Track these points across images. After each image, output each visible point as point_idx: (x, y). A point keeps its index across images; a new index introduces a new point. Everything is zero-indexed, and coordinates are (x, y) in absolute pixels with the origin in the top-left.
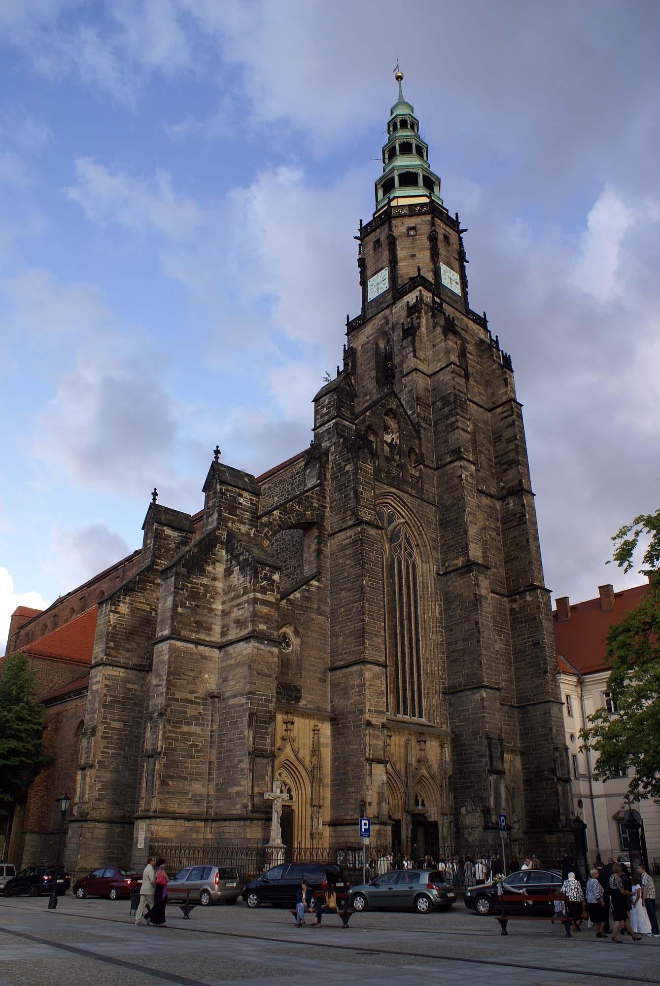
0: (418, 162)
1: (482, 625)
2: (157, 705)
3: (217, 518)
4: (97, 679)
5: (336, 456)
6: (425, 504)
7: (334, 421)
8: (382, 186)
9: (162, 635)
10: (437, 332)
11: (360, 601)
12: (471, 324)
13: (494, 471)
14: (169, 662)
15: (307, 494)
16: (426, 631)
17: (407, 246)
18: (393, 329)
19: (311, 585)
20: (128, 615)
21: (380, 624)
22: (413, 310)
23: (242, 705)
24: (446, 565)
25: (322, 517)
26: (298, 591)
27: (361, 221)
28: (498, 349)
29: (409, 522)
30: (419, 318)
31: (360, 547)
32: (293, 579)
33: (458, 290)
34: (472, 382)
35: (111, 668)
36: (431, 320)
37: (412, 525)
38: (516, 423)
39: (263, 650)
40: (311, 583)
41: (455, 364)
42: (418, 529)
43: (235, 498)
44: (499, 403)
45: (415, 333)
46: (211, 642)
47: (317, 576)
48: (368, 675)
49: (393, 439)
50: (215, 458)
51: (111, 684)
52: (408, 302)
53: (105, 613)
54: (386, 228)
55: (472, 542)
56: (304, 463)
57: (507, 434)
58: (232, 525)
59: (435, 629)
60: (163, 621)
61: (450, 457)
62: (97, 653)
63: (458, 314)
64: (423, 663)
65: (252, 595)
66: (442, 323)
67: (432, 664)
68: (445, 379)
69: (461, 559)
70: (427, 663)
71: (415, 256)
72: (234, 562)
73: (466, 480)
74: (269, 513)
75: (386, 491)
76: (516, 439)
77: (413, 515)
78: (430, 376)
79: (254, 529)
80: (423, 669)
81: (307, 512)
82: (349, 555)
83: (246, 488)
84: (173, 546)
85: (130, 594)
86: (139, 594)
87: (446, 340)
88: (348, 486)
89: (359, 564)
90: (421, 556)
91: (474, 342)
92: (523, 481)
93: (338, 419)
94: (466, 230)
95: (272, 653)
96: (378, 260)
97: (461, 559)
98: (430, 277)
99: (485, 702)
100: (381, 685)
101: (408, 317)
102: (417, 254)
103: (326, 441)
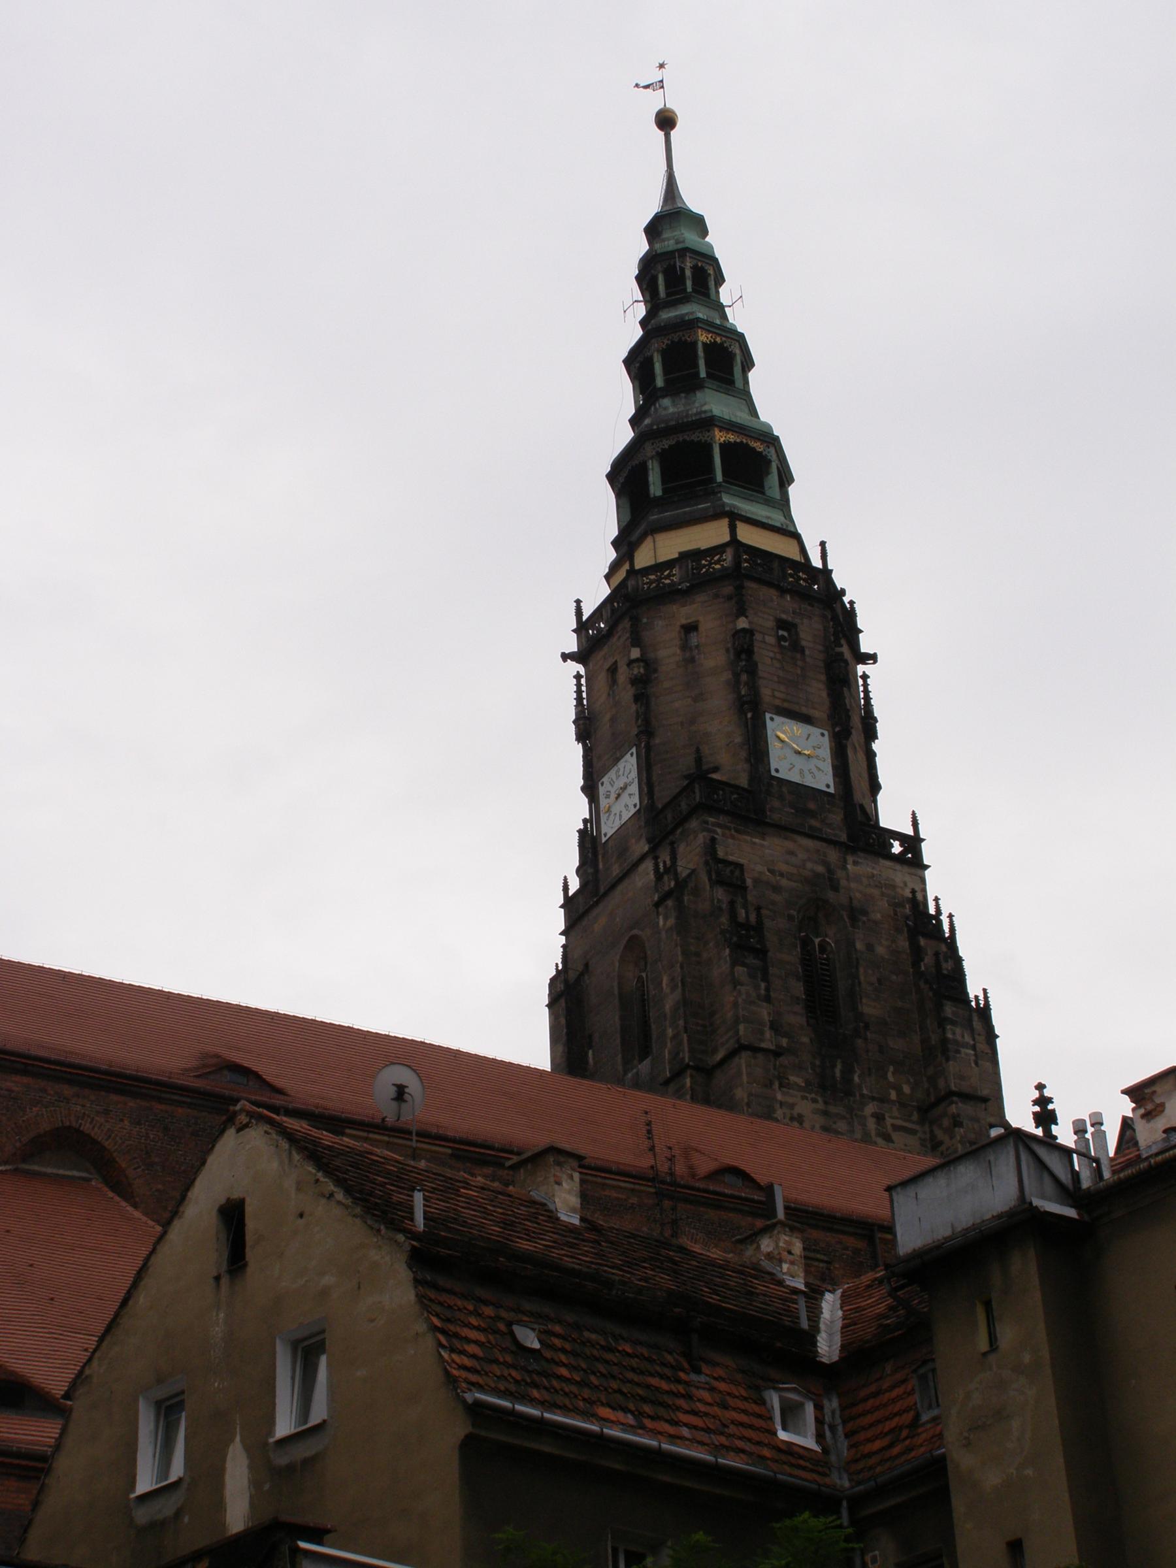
27: (578, 602)
33: (822, 778)
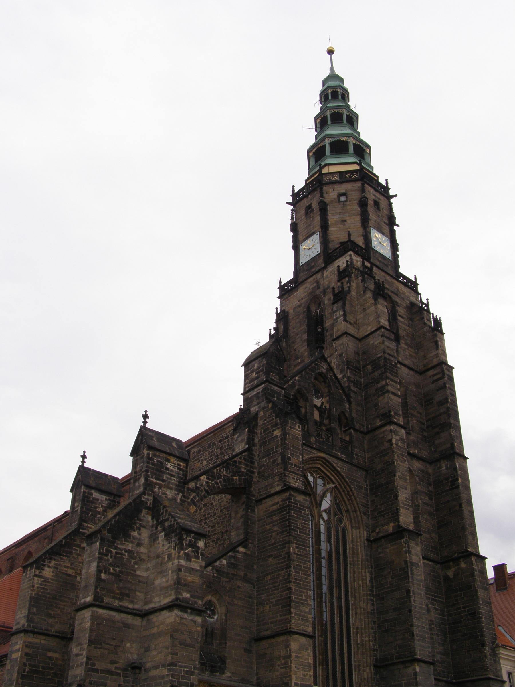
0: (348, 131)
1: (414, 593)
2: (76, 676)
3: (144, 484)
4: (17, 647)
5: (265, 420)
6: (355, 468)
7: (263, 385)
8: (314, 153)
9: (85, 601)
10: (368, 295)
11: (286, 568)
12: (402, 287)
13: (425, 434)
14: (91, 631)
15: (235, 459)
16: (356, 600)
17: (338, 211)
18: (324, 292)
19: (238, 552)
20: (52, 579)
21: (307, 593)
22: (343, 274)
23: (163, 677)
24: (377, 530)
25: (249, 483)
26: (225, 557)
27: (293, 187)
28: (428, 311)
29: (339, 487)
30: (349, 282)
31: (287, 513)
32: (220, 545)
34: (403, 345)
35: (32, 635)
36: (361, 284)
37: (341, 490)
38: (447, 385)
39: (186, 619)
40: (237, 549)
41: (385, 328)
42: (348, 494)
43: (162, 463)
44: (431, 365)
45: (346, 297)
46: (134, 609)
47: (244, 543)
48: (294, 646)
49: (322, 404)
50: (143, 422)
51: (31, 652)
52: (338, 267)
53: (30, 577)
54: (317, 194)
55: (403, 507)
56: (232, 428)
57: (438, 398)
58: (159, 490)
59: (365, 597)
60: (86, 587)
61: (380, 421)
62: (19, 618)
63: (388, 278)
64: (354, 633)
65: (176, 562)
66: (372, 286)
67: (362, 634)
68: (376, 343)
69: (392, 524)
70: (357, 633)
71: (345, 221)
72: (159, 528)
73: (397, 445)
74: (197, 478)
75: (315, 455)
76: (448, 402)
77: (343, 480)
78: (360, 340)
79: (181, 494)
80: (354, 640)
81: (235, 478)
82: (276, 521)
83: (173, 453)
84: (100, 509)
85: (56, 558)
86: (64, 558)
87: (375, 304)
88: (277, 451)
89: (286, 530)
90: (351, 522)
91: (405, 305)
92: (456, 444)
93: (267, 383)
94: (396, 196)
95: (195, 622)
96: (310, 225)
97: (392, 524)
98: (360, 242)
99: (418, 677)
100: (308, 657)
101: (338, 281)
102: (347, 219)
103: (255, 406)
